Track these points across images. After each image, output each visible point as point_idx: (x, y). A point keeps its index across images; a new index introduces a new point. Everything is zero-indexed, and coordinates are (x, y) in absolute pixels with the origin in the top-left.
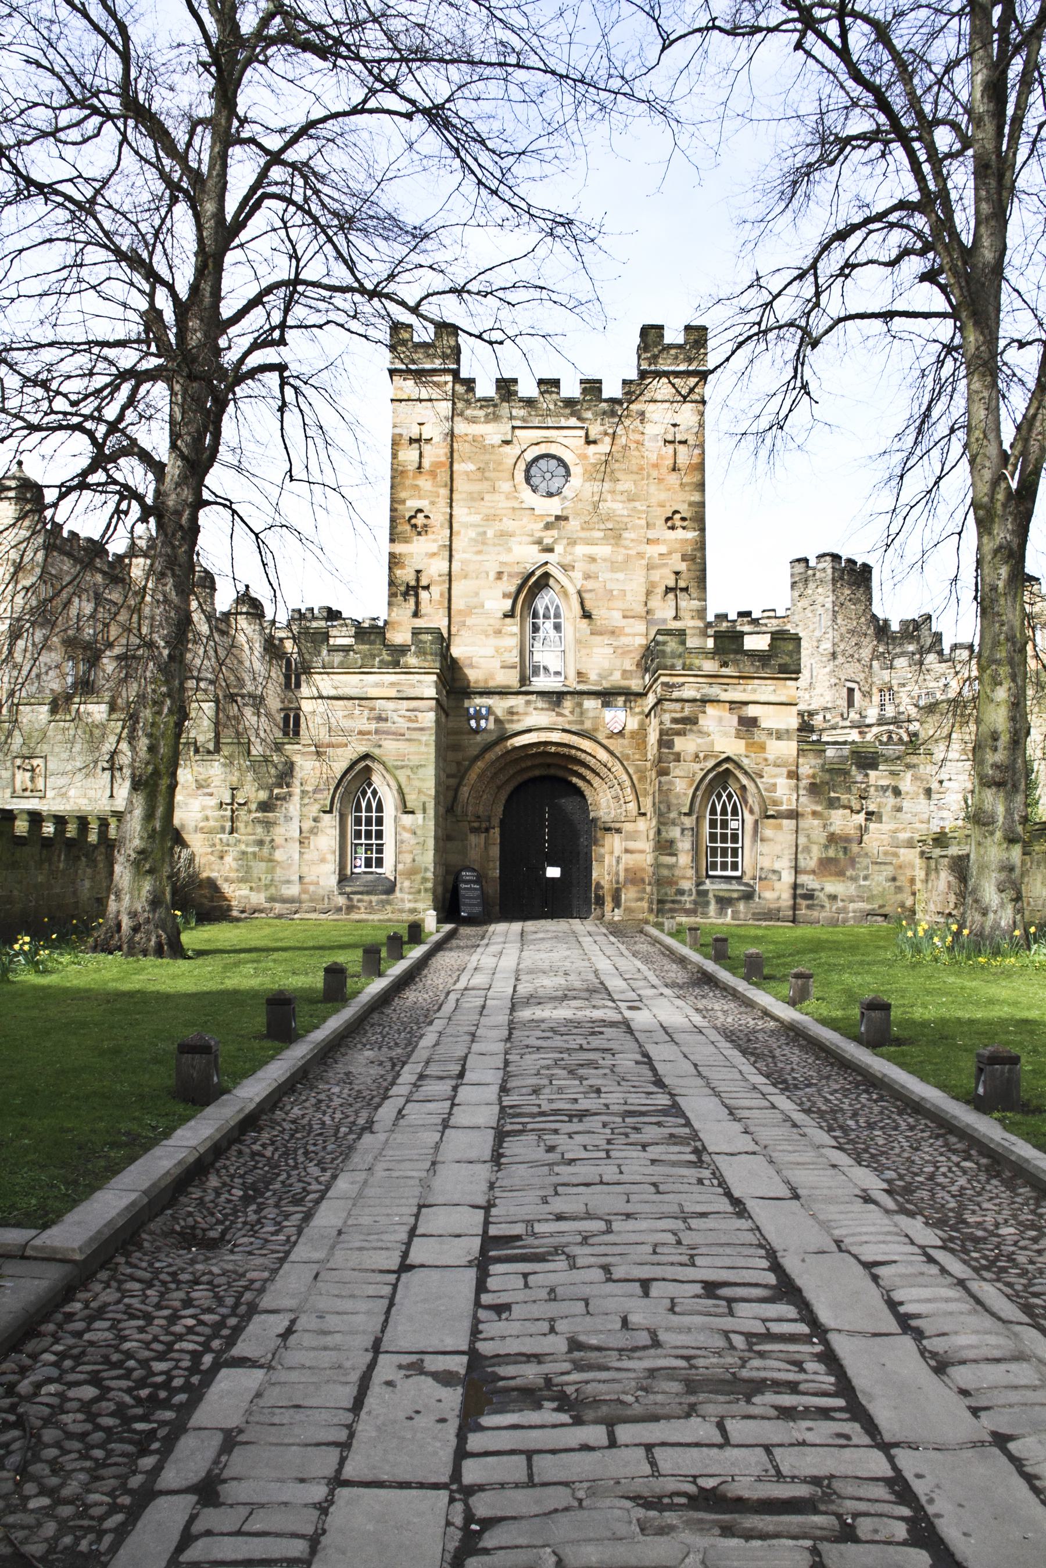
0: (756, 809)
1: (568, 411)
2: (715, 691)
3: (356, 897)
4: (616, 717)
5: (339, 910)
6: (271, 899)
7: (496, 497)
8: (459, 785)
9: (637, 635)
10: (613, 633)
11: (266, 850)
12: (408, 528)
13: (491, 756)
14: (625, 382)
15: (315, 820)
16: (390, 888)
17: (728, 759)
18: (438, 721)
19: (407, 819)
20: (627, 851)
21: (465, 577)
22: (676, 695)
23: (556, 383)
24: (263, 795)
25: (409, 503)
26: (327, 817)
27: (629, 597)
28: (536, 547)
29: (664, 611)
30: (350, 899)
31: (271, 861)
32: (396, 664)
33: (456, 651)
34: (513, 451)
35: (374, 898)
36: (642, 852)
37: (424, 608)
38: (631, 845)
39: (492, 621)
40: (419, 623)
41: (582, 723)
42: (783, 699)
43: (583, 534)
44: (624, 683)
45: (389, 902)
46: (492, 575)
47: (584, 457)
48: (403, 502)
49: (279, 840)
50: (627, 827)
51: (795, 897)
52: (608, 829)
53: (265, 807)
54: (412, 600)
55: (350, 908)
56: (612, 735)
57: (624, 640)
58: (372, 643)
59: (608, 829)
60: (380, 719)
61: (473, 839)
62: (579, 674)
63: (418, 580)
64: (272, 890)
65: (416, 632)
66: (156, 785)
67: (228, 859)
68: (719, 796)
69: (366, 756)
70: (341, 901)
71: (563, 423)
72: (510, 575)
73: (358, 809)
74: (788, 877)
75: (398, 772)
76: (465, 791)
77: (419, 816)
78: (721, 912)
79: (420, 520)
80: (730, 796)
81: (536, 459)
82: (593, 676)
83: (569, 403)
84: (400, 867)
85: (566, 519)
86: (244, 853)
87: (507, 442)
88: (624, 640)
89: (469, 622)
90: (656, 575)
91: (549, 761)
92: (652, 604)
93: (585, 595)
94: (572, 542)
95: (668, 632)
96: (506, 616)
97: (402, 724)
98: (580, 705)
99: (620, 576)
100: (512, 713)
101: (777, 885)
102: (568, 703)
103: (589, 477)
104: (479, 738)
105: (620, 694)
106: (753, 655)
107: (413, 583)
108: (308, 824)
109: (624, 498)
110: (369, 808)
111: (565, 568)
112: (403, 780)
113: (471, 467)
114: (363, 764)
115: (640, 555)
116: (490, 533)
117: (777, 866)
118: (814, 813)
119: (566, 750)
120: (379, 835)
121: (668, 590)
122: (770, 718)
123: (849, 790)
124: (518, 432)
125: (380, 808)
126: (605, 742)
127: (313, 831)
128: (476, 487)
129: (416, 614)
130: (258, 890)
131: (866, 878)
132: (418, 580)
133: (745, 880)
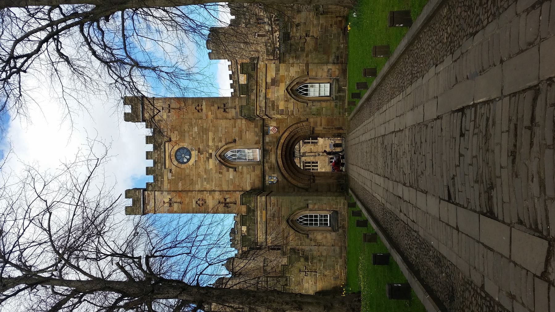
0: (305, 78)
2: (262, 94)
4: (272, 129)
5: (344, 231)
6: (341, 257)
7: (191, 174)
8: (297, 186)
9: (242, 123)
11: (323, 259)
12: (203, 207)
13: (287, 175)
14: (147, 127)
15: (311, 240)
16: (336, 212)
17: (287, 89)
18: (274, 195)
19: (311, 206)
20: (321, 125)
22: (264, 109)
23: (148, 153)
24: (302, 260)
25: (194, 206)
26: (310, 236)
27: (228, 126)
29: (232, 113)
31: (326, 257)
32: (254, 211)
33: (248, 188)
35: (339, 219)
36: (321, 120)
37: (232, 200)
38: (319, 124)
39: (237, 176)
40: (239, 202)
41: (274, 142)
42: (264, 69)
43: (205, 143)
44: (259, 126)
45: (341, 213)
46: (220, 176)
47: (176, 143)
49: (319, 254)
50: (312, 125)
51: (337, 63)
52: (313, 131)
53: (306, 259)
54: (231, 205)
55: (343, 227)
56: (278, 131)
57: (244, 127)
58: (246, 219)
59: (313, 131)
60: (274, 216)
61: (316, 182)
62: (256, 143)
64: (337, 256)
65: (242, 204)
66: (300, 302)
67: (326, 273)
68: (300, 92)
69: (287, 221)
70: (341, 231)
71: (163, 150)
73: (307, 224)
74: (330, 66)
75: (293, 210)
76: (300, 185)
77: (309, 202)
78: (344, 91)
79: (200, 202)
80: (301, 88)
81: (177, 160)
82: (257, 138)
83: (155, 148)
84: (328, 209)
85: (199, 149)
86: (324, 267)
87: (171, 171)
88: (244, 127)
90: (219, 116)
91: (288, 154)
93: (228, 141)
94: (208, 146)
95: (241, 112)
96: (235, 171)
97: (276, 208)
98: (267, 143)
99: (220, 128)
100: (271, 168)
101: (333, 70)
102: (267, 147)
103: (184, 141)
104: (280, 180)
105: (263, 128)
106: (248, 79)
107: (224, 204)
108: (313, 244)
109: (191, 128)
111: (218, 149)
112: (296, 208)
113: (180, 184)
114: (290, 223)
116: (205, 177)
117: (326, 70)
119: (284, 148)
120: (316, 216)
121: (225, 111)
122: (272, 74)
123: (298, 44)
124: (167, 167)
125: (306, 216)
126: (281, 134)
127: (315, 241)
129: (235, 204)
130: (337, 262)
131: (331, 36)
132: (222, 203)
133: (331, 82)
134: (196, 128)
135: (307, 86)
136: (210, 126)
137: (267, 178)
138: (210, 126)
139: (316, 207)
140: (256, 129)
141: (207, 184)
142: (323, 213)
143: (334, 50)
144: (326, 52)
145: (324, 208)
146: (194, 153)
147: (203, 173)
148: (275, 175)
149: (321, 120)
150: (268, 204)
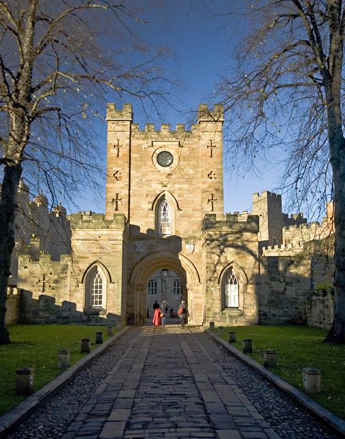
1: (172, 136)
3: (91, 316)
9: (199, 218)
10: (189, 216)
19: (111, 286)
21: (135, 196)
28: (161, 185)
30: (89, 317)
32: (108, 227)
34: (152, 150)
36: (200, 298)
38: (197, 295)
40: (117, 212)
46: (145, 195)
47: (178, 152)
48: (112, 168)
51: (259, 315)
54: (115, 204)
55: (89, 321)
58: (98, 219)
60: (101, 248)
63: (117, 197)
70: (85, 318)
71: (171, 140)
72: (151, 195)
88: (193, 219)
89: (136, 212)
92: (204, 206)
94: (174, 184)
96: (150, 210)
100: (152, 246)
108: (73, 288)
110: (97, 282)
114: (94, 265)
115: (199, 188)
116: (144, 180)
118: (266, 283)
120: (101, 292)
125: (101, 282)
127: (75, 291)
128: (138, 163)
129: (116, 210)
130: (52, 314)
132: (117, 197)
134: (193, 172)
135: (235, 283)
136: (193, 185)
137: (142, 242)
138: (193, 185)
139: (111, 292)
140: (191, 232)
141: (137, 182)
142: (104, 300)
143: (272, 311)
144: (271, 303)
145: (108, 301)
146: (167, 170)
147: (147, 178)
148: (144, 251)
149: (200, 298)
150: (114, 242)
